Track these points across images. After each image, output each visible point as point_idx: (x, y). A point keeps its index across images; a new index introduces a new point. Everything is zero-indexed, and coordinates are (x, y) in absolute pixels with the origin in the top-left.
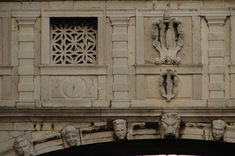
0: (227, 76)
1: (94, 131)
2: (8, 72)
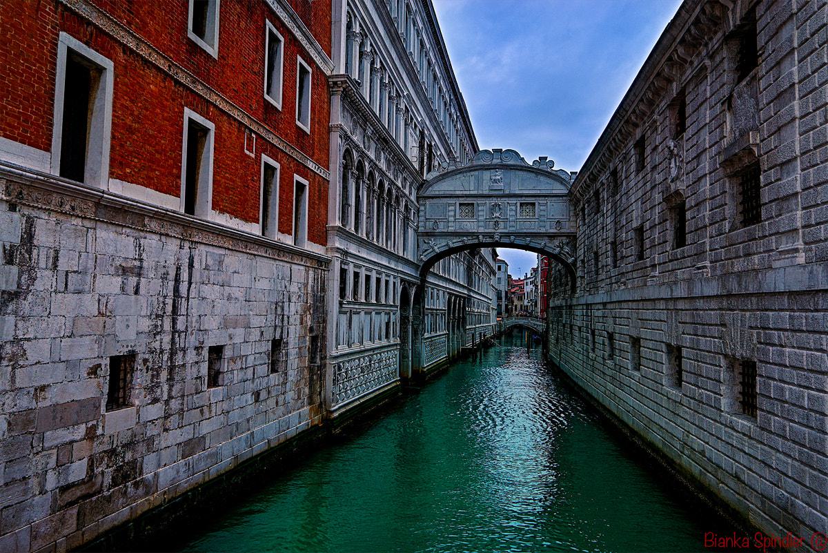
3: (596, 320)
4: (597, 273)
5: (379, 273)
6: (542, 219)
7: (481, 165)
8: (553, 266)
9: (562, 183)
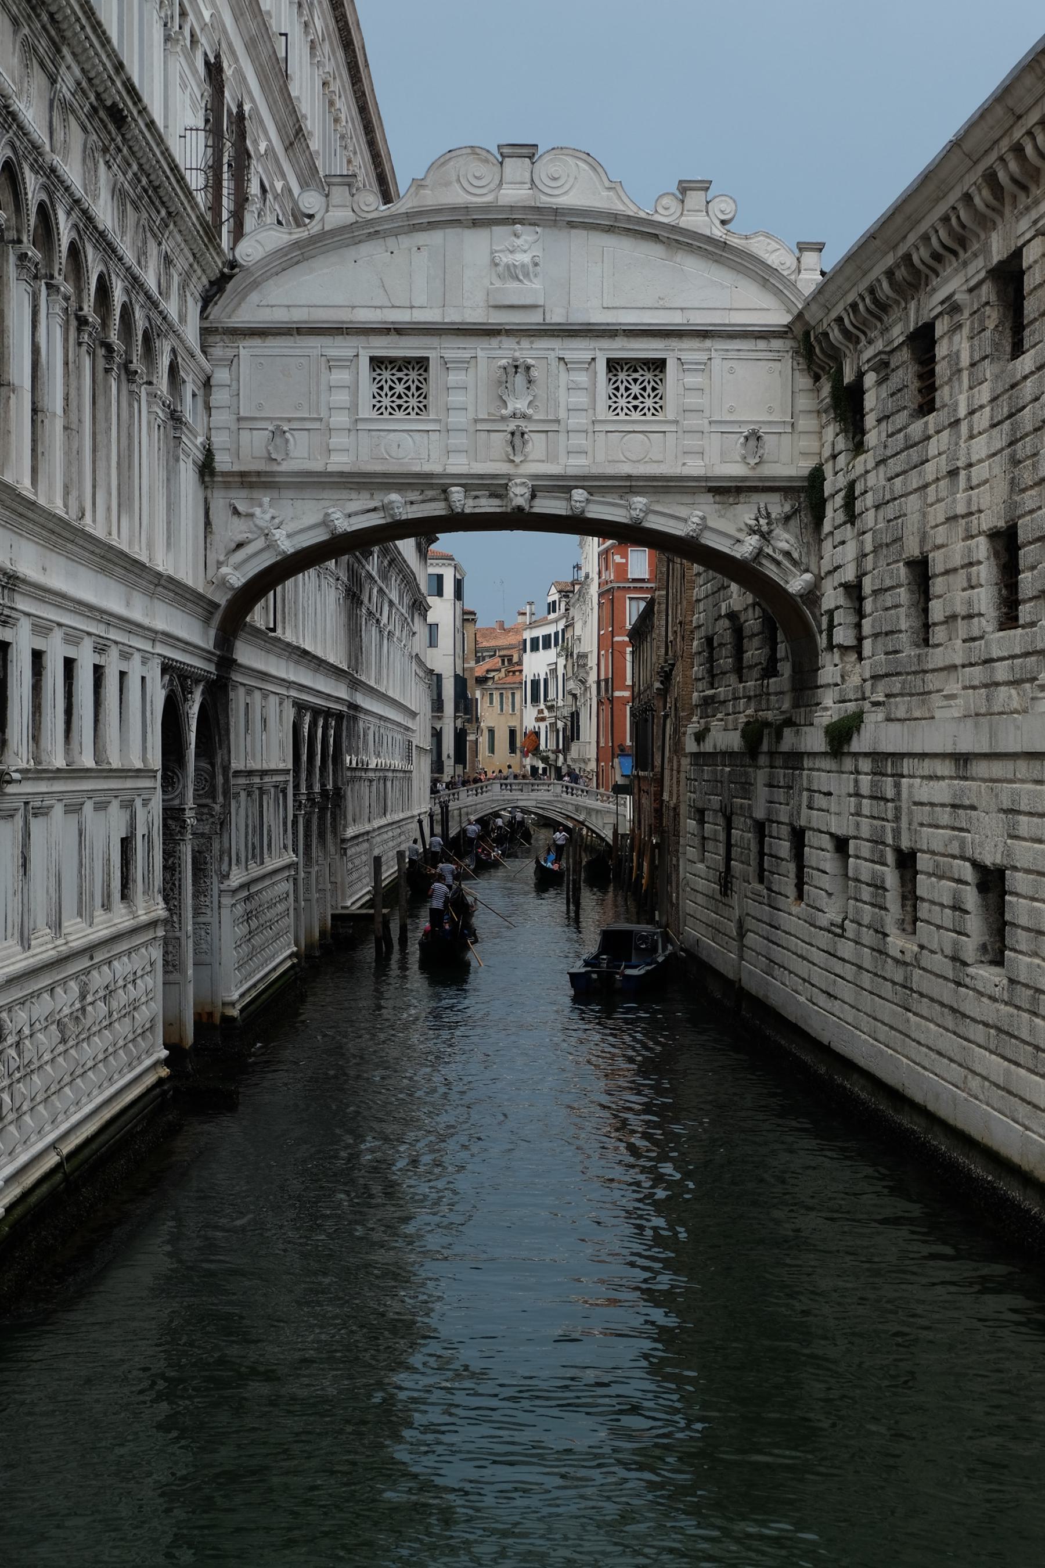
0: (590, 434)
1: (423, 501)
2: (316, 425)
3: (922, 814)
4: (924, 636)
5: (100, 649)
6: (692, 422)
7: (454, 209)
8: (699, 592)
9: (764, 283)
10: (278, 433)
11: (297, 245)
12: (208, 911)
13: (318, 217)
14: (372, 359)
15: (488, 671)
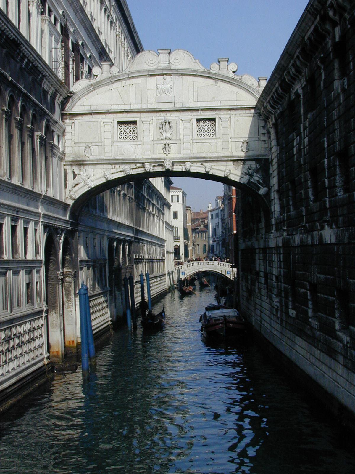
1: (136, 168)
2: (100, 144)
5: (15, 219)
7: (144, 71)
10: (88, 147)
11: (91, 85)
12: (71, 307)
13: (99, 76)
14: (118, 121)
15: (197, 226)
